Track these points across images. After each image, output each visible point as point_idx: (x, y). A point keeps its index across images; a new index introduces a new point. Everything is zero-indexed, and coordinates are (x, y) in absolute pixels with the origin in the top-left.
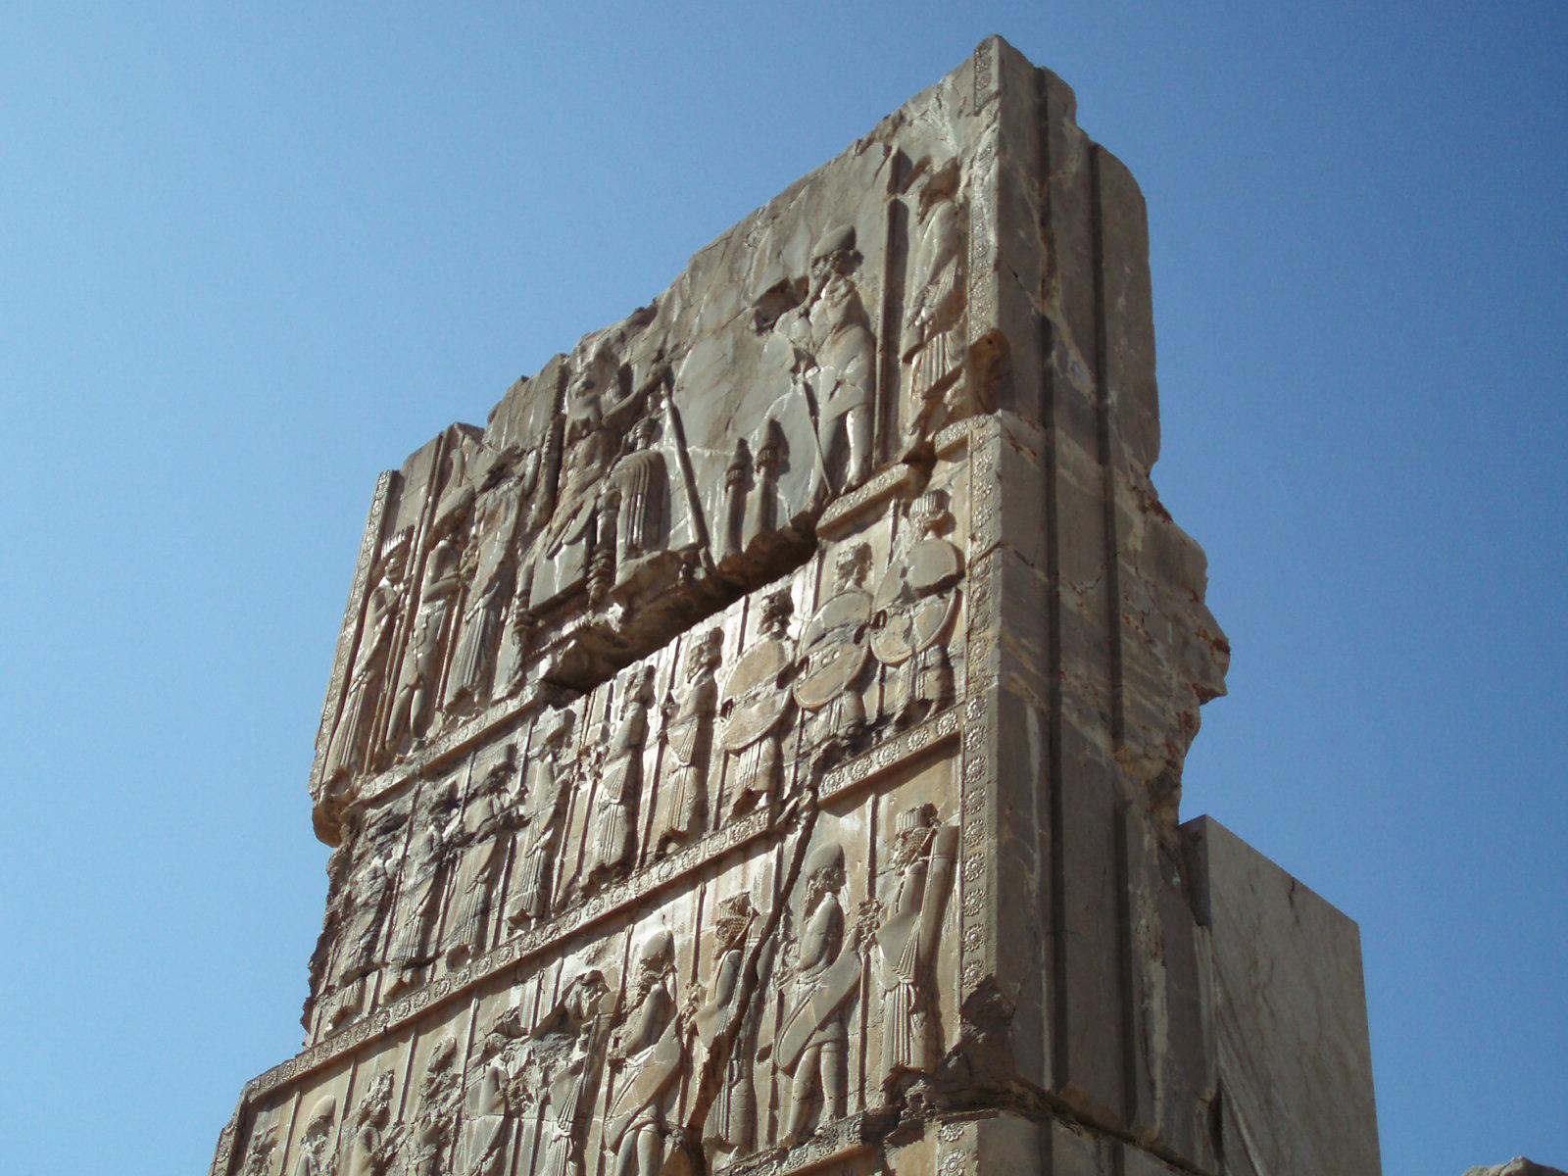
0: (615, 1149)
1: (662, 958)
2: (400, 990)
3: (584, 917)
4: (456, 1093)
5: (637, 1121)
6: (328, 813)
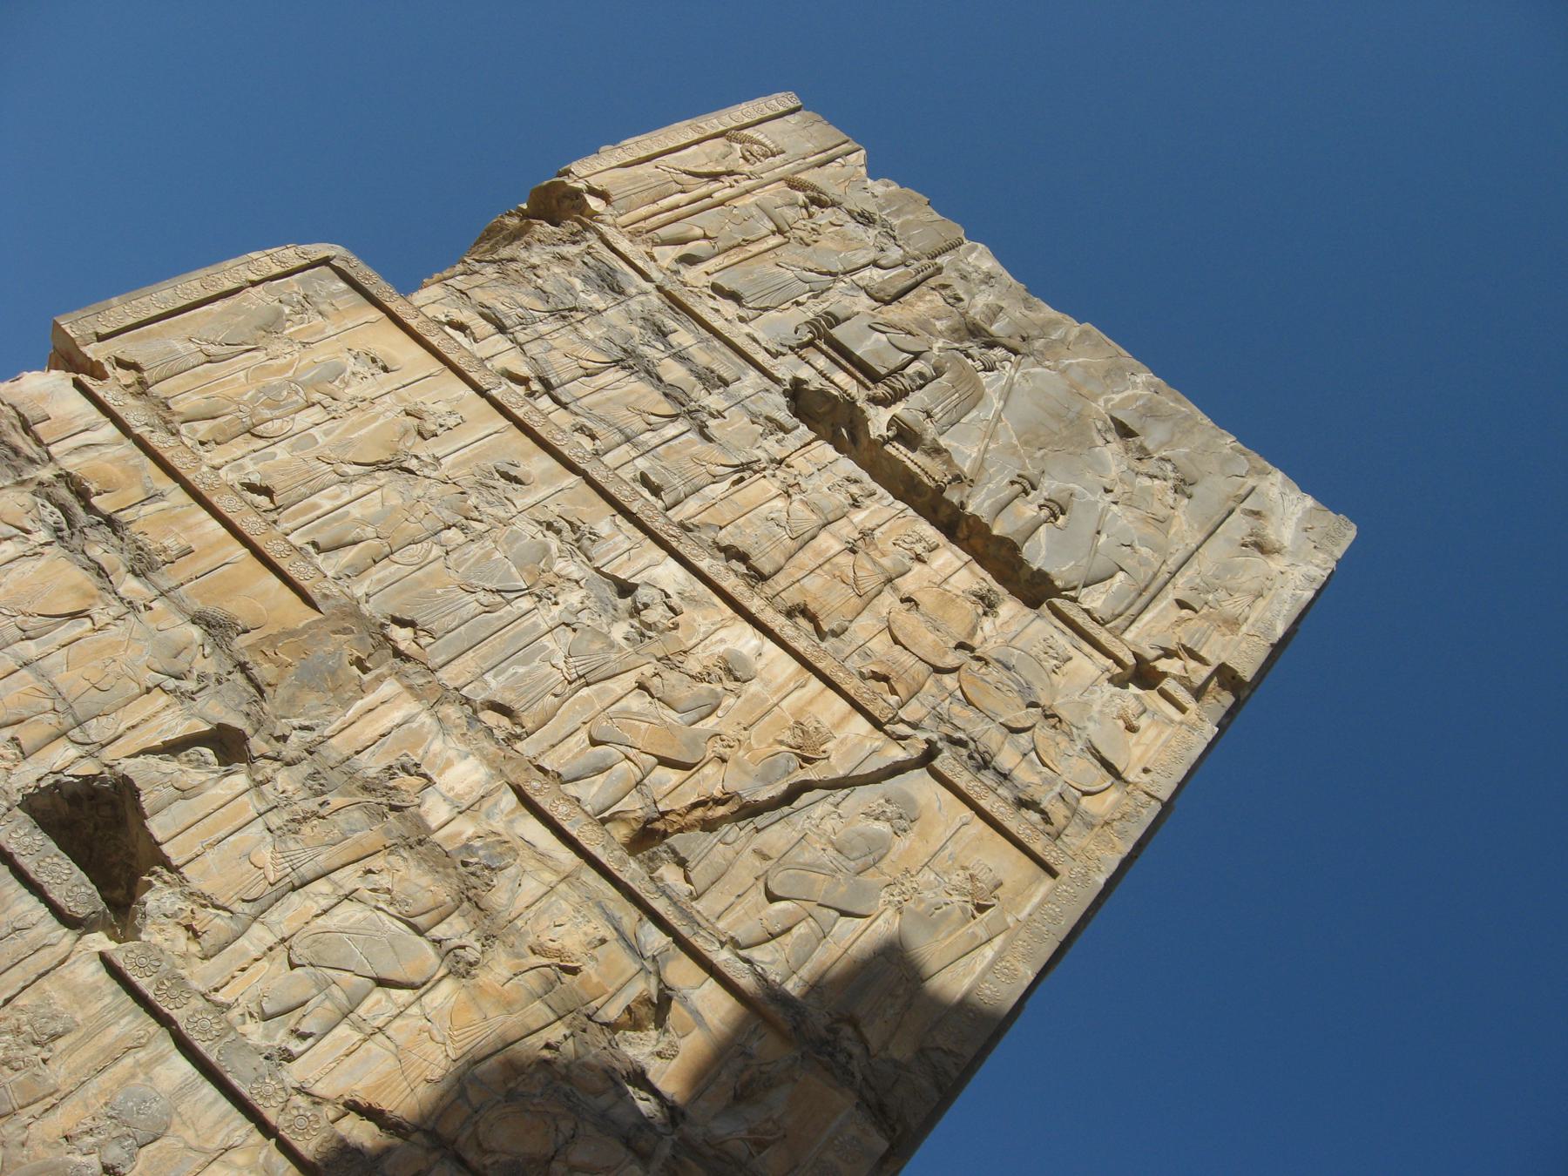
0: (594, 743)
1: (733, 671)
3: (704, 564)
4: (501, 514)
5: (631, 752)
6: (565, 196)
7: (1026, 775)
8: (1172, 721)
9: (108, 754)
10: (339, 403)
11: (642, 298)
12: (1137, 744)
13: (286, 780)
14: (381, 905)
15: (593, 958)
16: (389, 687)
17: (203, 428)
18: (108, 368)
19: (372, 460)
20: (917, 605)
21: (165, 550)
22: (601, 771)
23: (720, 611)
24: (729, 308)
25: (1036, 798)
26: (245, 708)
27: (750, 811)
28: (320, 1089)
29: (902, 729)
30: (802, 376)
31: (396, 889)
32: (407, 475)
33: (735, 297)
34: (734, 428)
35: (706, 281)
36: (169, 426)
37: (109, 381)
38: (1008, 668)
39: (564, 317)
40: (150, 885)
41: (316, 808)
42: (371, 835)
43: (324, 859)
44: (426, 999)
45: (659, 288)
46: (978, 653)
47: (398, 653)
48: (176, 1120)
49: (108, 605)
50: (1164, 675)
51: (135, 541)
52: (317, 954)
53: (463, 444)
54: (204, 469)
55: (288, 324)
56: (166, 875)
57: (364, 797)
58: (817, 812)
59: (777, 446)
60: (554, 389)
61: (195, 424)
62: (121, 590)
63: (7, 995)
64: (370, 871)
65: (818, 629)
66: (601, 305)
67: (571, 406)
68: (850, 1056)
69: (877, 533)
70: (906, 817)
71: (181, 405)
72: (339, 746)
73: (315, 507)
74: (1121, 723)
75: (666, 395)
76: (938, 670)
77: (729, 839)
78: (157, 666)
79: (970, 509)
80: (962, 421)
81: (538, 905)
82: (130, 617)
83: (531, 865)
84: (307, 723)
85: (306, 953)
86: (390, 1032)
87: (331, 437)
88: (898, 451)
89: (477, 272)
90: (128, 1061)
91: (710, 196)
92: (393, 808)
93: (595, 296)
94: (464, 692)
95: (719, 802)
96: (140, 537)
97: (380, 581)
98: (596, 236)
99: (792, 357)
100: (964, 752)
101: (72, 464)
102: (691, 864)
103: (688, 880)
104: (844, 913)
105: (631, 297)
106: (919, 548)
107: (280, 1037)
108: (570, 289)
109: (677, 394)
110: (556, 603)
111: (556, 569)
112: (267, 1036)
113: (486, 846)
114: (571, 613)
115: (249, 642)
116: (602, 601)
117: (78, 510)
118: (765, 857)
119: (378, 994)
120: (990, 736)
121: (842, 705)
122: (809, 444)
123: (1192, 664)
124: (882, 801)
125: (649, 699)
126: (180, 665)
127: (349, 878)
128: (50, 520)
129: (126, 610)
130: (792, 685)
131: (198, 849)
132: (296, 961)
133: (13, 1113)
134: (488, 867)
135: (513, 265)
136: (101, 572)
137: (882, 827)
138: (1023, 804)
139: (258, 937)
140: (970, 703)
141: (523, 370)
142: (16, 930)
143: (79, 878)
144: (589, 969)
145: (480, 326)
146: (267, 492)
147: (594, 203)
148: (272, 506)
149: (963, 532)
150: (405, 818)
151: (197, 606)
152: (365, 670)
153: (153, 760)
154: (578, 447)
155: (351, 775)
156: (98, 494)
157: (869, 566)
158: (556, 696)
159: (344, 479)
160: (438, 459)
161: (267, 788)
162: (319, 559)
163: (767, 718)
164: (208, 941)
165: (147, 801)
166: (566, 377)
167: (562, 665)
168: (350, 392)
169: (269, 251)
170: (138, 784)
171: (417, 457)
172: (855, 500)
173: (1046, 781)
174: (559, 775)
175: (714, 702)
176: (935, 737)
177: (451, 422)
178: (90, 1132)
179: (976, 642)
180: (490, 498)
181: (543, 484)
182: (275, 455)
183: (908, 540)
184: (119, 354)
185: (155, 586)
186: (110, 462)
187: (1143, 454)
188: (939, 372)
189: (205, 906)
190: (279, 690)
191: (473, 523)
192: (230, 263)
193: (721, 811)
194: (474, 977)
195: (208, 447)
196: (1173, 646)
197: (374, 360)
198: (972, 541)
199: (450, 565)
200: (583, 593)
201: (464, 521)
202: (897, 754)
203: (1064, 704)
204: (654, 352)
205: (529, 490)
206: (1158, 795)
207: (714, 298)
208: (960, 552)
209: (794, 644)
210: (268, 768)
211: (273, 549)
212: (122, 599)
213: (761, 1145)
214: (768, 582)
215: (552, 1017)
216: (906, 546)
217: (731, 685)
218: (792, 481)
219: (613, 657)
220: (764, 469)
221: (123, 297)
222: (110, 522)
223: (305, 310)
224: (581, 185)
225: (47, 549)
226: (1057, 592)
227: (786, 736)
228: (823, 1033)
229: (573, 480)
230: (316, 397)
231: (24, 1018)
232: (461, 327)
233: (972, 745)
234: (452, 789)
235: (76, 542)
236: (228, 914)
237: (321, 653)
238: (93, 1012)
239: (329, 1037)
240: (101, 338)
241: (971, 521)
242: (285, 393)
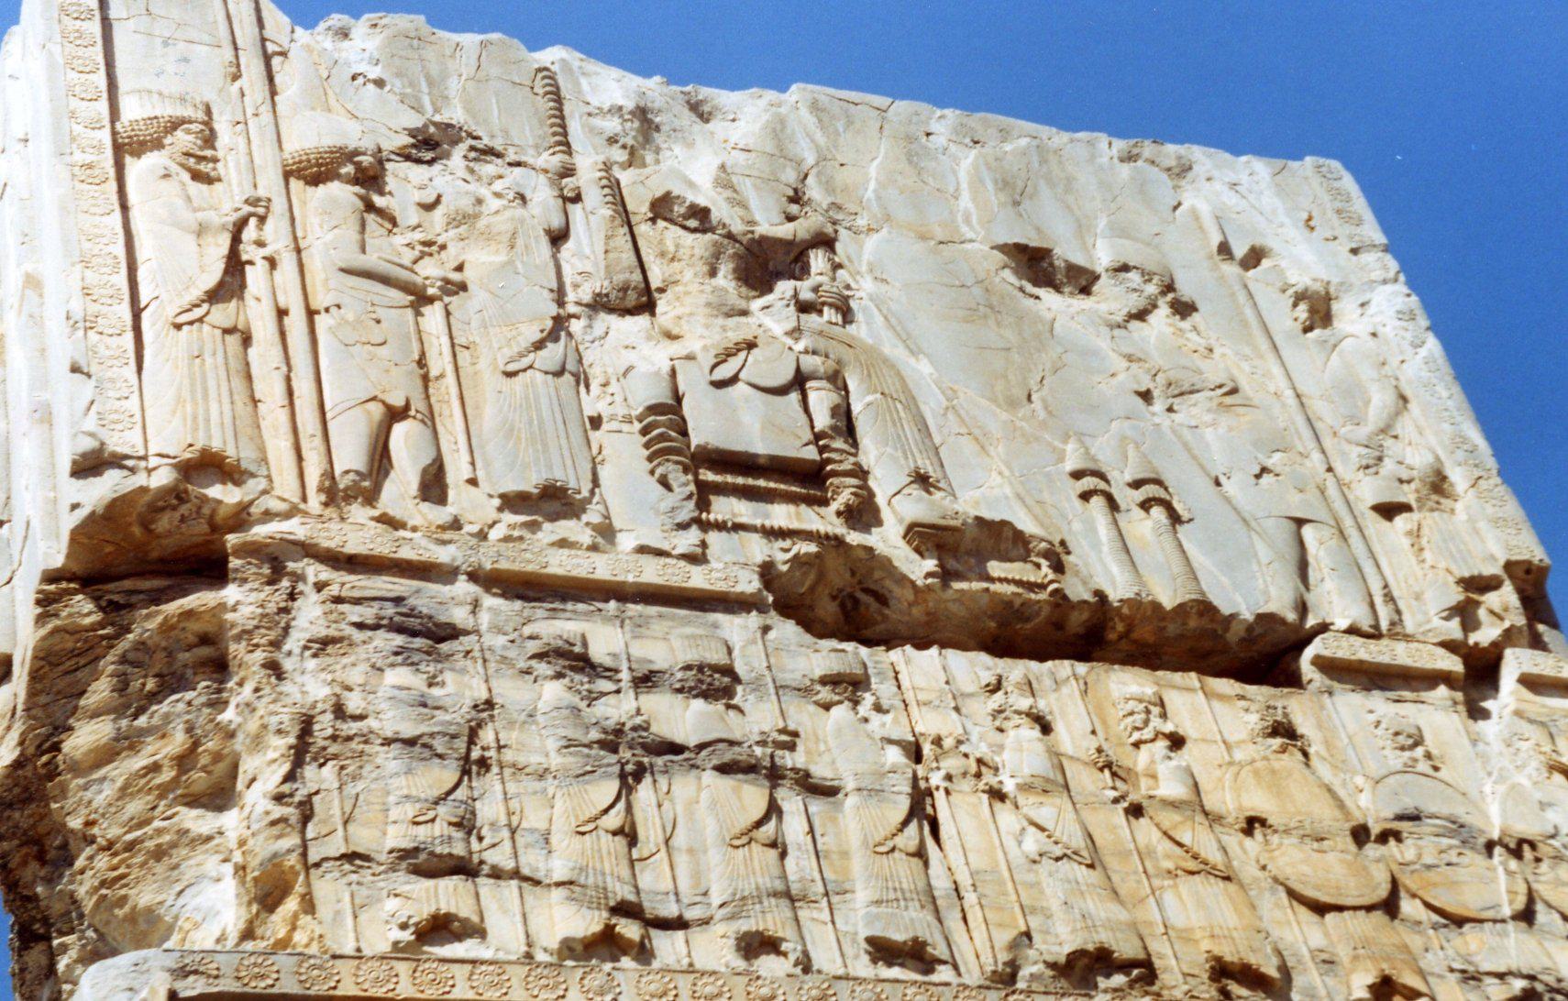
67: (690, 915)
75: (724, 769)
80: (937, 440)
91: (282, 313)
109: (728, 755)
123: (1492, 599)
140: (1459, 921)
141: (587, 923)
145: (448, 895)
147: (224, 494)
187: (1082, 280)
188: (836, 380)
196: (1456, 595)
216: (1147, 734)
218: (973, 768)
224: (162, 478)
232: (439, 928)
241: (1125, 611)
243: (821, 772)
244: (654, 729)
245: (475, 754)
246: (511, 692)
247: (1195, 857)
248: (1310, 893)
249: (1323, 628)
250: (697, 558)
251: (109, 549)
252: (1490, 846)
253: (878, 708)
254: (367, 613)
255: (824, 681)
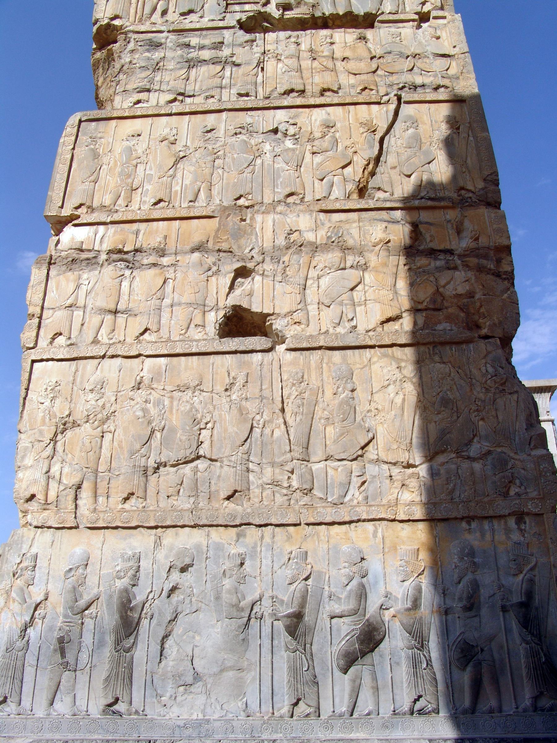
0: (322, 180)
1: (329, 126)
2: (175, 100)
5: (334, 173)
7: (428, 80)
8: (445, 24)
9: (221, 305)
10: (142, 158)
11: (169, 40)
12: (444, 41)
13: (268, 266)
14: (328, 272)
15: (389, 234)
16: (259, 218)
17: (120, 201)
18: (76, 213)
19: (172, 164)
20: (348, 58)
21: (160, 243)
22: (332, 185)
23: (305, 112)
24: (192, 17)
25: (438, 84)
26: (234, 260)
27: (377, 160)
28: (371, 327)
29: (385, 99)
30: (238, 18)
31: (327, 265)
32: (185, 158)
33: (191, 12)
34: (241, 55)
35: (176, 15)
36: (113, 211)
37: (82, 216)
38: (390, 53)
39: (158, 69)
40: (271, 324)
41: (283, 265)
42: (304, 259)
43: (302, 274)
44: (366, 283)
45: (169, 32)
46: (378, 56)
47: (247, 207)
48: (351, 366)
49: (168, 271)
50: (429, 12)
51: (150, 249)
52: (330, 298)
53: (186, 135)
54: (139, 212)
55: (98, 150)
56: (273, 317)
57: (290, 251)
58: (391, 142)
59: (258, 48)
60: (185, 94)
61: (117, 203)
62: (165, 264)
63: (280, 380)
64: (315, 267)
65: (333, 91)
66: (162, 55)
67: (195, 94)
68: (470, 198)
69: (313, 47)
70: (414, 122)
71: (107, 200)
72: (268, 245)
73: (176, 192)
74: (434, 39)
75: (213, 64)
76: (374, 72)
77: (383, 172)
78: (201, 272)
79: (327, 14)
81: (361, 234)
82: (177, 268)
83: (347, 226)
84: (250, 248)
85: (328, 300)
86: (368, 299)
87: (153, 169)
88: (289, 14)
89: (119, 81)
90: (324, 365)
92: (301, 246)
93: (157, 53)
94: (276, 200)
95: (368, 165)
96: (149, 246)
97: (218, 193)
98: (132, 34)
99: (228, 15)
100: (406, 89)
101: (106, 247)
102: (382, 187)
103: (386, 192)
104: (429, 163)
105: (166, 43)
106: (329, 40)
107: (348, 325)
108: (149, 59)
109: (216, 60)
110: (266, 153)
111: (253, 144)
112: (344, 328)
113: (332, 233)
114: (272, 152)
115: (212, 243)
116: (275, 141)
117: (125, 256)
118: (395, 168)
119: (355, 293)
120: (407, 78)
121: (364, 107)
122: (265, 38)
124: (404, 124)
125: (319, 155)
126: (206, 267)
127: (313, 273)
128: (123, 266)
129: (174, 268)
130: (347, 115)
131: (272, 304)
132: (328, 305)
133: (317, 402)
134: (339, 237)
135: (125, 68)
136: (155, 265)
137: (411, 131)
138: (436, 89)
139: (312, 309)
140: (392, 73)
141: (171, 97)
142: (261, 365)
143: (258, 339)
144: (391, 237)
146: (160, 201)
148: (167, 203)
149: (330, 23)
150: (306, 246)
151: (188, 248)
152: (245, 220)
153: (231, 295)
154: (212, 104)
155: (279, 249)
156: (124, 247)
157: (324, 59)
158: (298, 177)
159: (173, 176)
160: (186, 146)
161: (266, 273)
162: (196, 204)
163: (352, 130)
164: (304, 321)
165: (245, 305)
166: (183, 86)
167: (289, 168)
168: (140, 151)
169: (64, 135)
170: (238, 304)
171: (180, 151)
172: (297, 43)
173: (435, 76)
174: (325, 197)
175: (335, 139)
176: (395, 92)
177: (174, 131)
178: (338, 388)
179: (374, 54)
180: (213, 142)
181: (219, 123)
182: (147, 190)
183: (323, 40)
184: (73, 206)
185: (171, 254)
186: (114, 235)
189: (292, 315)
190: (234, 247)
191: (219, 153)
192: (60, 150)
193: (371, 166)
194: (370, 266)
195: (129, 205)
197: (133, 136)
198: (336, 23)
199: (228, 171)
200: (268, 144)
201: (216, 155)
202: (392, 107)
203: (415, 49)
204: (193, 54)
205: (218, 130)
206: (465, 51)
207: (186, 18)
208: (339, 30)
209: (334, 102)
210: (259, 268)
211: (184, 214)
212: (168, 266)
213: (477, 239)
214: (306, 91)
215: (398, 257)
216: (324, 43)
217: (333, 130)
218: (276, 55)
219: (298, 152)
220: (264, 59)
221: (50, 190)
222: (136, 251)
223: (96, 142)
225: (134, 274)
226: (376, 16)
227: (362, 130)
228: (459, 198)
229: (224, 114)
230: (134, 162)
231: (291, 380)
232: (139, 102)
233: (407, 85)
234: (306, 227)
235: (137, 264)
236: (300, 311)
237: (231, 227)
238: (302, 364)
239: (357, 314)
240: (62, 207)
241: (331, 17)
242: (126, 170)
243: (238, 61)
244: (201, 58)
245: (157, 67)
246: (169, 54)
247: (326, 67)
248: (353, 72)
249: (383, 13)
250: (223, 19)
251: (101, 41)
252: (408, 57)
253: (257, 46)
254: (142, 43)
255: (245, 42)
